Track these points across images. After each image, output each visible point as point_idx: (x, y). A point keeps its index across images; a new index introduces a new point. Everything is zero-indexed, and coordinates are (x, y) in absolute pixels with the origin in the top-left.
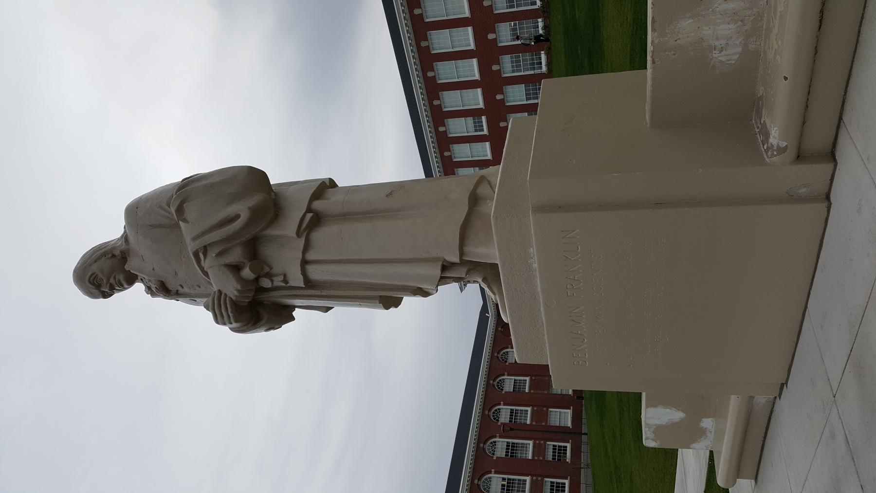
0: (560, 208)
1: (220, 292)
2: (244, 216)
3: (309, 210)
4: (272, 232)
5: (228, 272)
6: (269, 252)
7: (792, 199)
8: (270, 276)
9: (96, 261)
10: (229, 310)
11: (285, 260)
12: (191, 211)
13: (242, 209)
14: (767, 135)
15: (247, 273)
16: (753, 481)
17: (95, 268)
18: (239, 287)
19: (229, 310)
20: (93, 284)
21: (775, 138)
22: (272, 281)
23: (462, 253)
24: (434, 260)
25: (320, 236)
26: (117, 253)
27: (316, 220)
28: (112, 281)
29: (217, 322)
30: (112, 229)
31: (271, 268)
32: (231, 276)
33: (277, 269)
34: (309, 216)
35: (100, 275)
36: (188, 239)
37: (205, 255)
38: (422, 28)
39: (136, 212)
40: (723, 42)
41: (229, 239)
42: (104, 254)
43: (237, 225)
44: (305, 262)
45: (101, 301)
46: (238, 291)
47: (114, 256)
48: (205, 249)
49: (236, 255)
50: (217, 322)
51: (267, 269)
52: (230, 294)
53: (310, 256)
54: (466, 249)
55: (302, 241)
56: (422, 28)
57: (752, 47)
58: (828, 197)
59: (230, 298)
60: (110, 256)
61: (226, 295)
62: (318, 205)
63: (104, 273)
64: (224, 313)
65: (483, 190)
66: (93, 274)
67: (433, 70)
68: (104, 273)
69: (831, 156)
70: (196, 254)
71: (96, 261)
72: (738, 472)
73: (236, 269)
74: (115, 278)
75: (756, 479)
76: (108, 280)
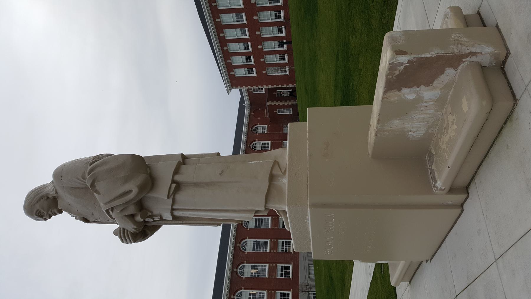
0: (324, 205)
1: (124, 229)
2: (135, 191)
3: (173, 182)
4: (151, 195)
5: (128, 220)
6: (150, 204)
7: (445, 206)
8: (152, 217)
9: (37, 202)
10: (130, 238)
11: (160, 202)
12: (100, 186)
13: (133, 187)
14: (435, 180)
15: (139, 219)
16: (408, 283)
17: (38, 207)
18: (135, 227)
19: (130, 238)
20: (39, 216)
21: (439, 184)
22: (153, 219)
23: (265, 206)
24: (250, 211)
25: (180, 197)
26: (50, 196)
27: (178, 187)
28: (50, 213)
29: (123, 242)
30: (45, 178)
31: (152, 212)
32: (130, 222)
33: (156, 212)
34: (174, 185)
35: (42, 211)
36: (102, 205)
37: (112, 211)
38: (216, 12)
39: (60, 174)
40: (415, 129)
41: (127, 203)
42: (42, 197)
43: (131, 196)
44: (173, 210)
45: (43, 222)
46: (135, 229)
47: (48, 198)
48: (112, 209)
49: (131, 210)
50: (123, 242)
51: (150, 214)
52: (129, 230)
53: (174, 207)
54: (267, 205)
55: (171, 200)
56: (216, 12)
57: (430, 131)
58: (462, 206)
59: (131, 232)
60: (46, 198)
61: (127, 231)
62: (178, 178)
63: (42, 205)
64: (127, 238)
65: (277, 172)
66: (38, 210)
67: (226, 46)
68: (42, 205)
69: (466, 189)
70: (107, 211)
71: (37, 202)
72: (402, 278)
73: (132, 217)
74: (51, 211)
75: (410, 282)
76: (48, 213)
